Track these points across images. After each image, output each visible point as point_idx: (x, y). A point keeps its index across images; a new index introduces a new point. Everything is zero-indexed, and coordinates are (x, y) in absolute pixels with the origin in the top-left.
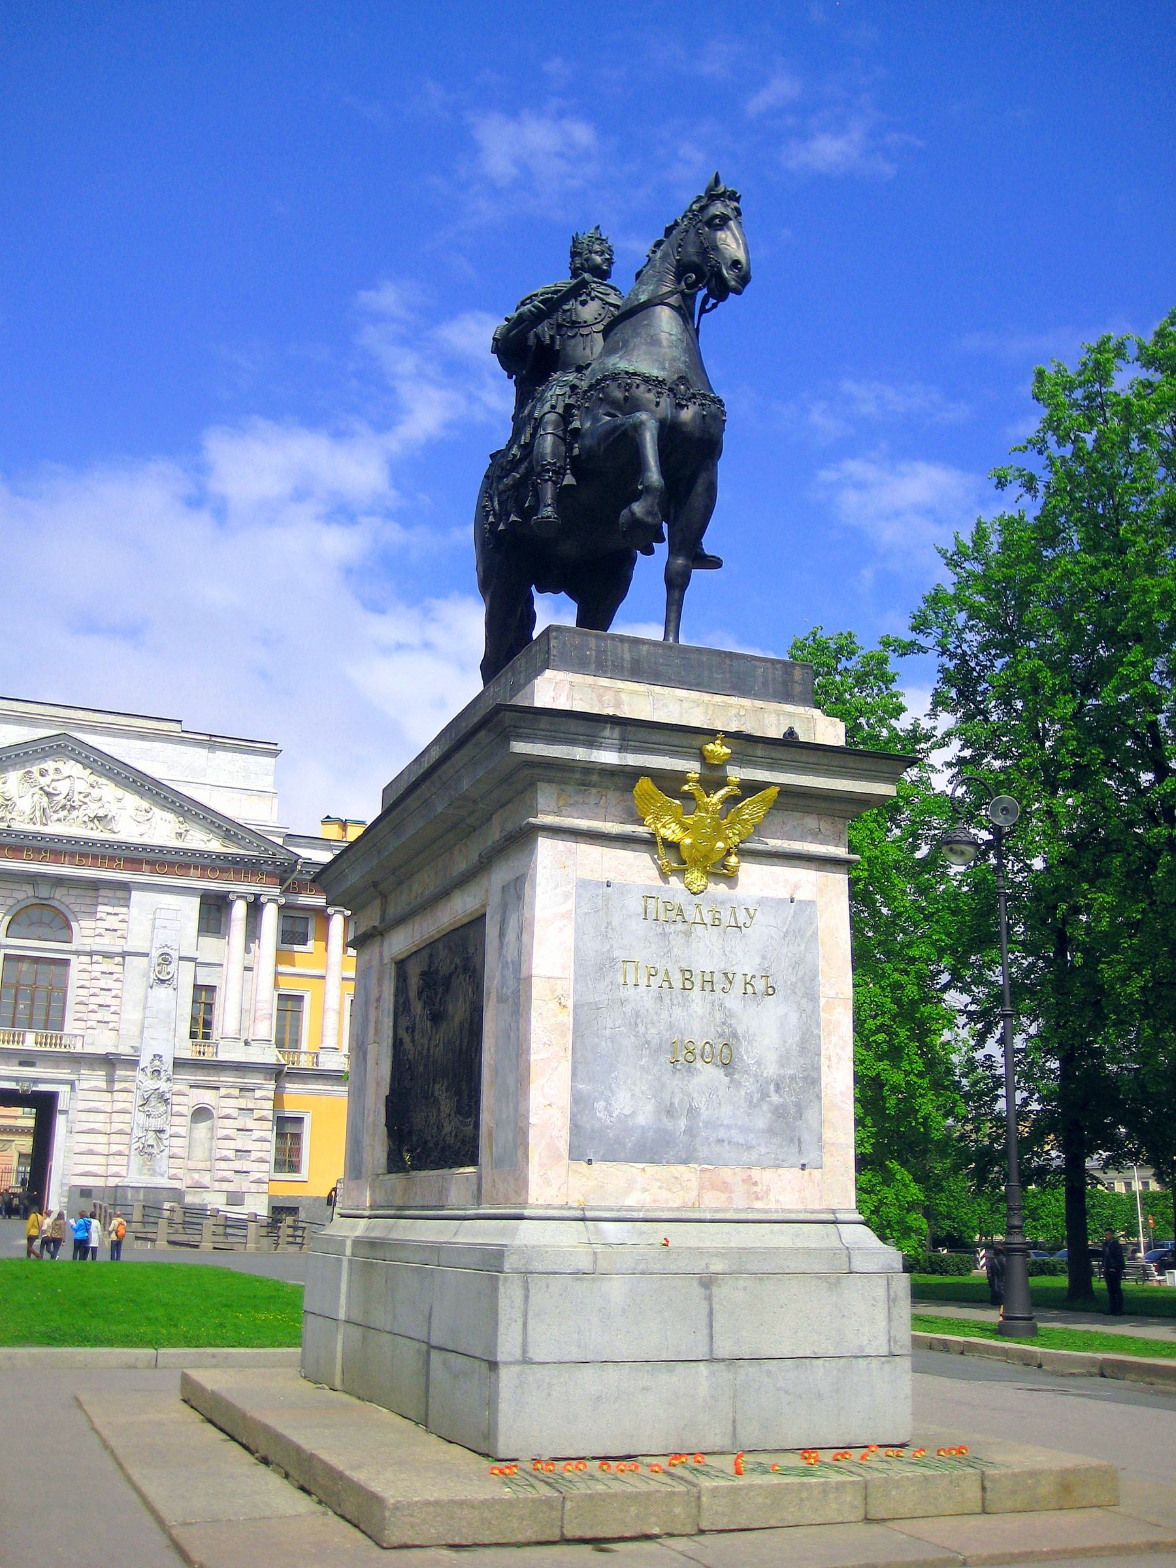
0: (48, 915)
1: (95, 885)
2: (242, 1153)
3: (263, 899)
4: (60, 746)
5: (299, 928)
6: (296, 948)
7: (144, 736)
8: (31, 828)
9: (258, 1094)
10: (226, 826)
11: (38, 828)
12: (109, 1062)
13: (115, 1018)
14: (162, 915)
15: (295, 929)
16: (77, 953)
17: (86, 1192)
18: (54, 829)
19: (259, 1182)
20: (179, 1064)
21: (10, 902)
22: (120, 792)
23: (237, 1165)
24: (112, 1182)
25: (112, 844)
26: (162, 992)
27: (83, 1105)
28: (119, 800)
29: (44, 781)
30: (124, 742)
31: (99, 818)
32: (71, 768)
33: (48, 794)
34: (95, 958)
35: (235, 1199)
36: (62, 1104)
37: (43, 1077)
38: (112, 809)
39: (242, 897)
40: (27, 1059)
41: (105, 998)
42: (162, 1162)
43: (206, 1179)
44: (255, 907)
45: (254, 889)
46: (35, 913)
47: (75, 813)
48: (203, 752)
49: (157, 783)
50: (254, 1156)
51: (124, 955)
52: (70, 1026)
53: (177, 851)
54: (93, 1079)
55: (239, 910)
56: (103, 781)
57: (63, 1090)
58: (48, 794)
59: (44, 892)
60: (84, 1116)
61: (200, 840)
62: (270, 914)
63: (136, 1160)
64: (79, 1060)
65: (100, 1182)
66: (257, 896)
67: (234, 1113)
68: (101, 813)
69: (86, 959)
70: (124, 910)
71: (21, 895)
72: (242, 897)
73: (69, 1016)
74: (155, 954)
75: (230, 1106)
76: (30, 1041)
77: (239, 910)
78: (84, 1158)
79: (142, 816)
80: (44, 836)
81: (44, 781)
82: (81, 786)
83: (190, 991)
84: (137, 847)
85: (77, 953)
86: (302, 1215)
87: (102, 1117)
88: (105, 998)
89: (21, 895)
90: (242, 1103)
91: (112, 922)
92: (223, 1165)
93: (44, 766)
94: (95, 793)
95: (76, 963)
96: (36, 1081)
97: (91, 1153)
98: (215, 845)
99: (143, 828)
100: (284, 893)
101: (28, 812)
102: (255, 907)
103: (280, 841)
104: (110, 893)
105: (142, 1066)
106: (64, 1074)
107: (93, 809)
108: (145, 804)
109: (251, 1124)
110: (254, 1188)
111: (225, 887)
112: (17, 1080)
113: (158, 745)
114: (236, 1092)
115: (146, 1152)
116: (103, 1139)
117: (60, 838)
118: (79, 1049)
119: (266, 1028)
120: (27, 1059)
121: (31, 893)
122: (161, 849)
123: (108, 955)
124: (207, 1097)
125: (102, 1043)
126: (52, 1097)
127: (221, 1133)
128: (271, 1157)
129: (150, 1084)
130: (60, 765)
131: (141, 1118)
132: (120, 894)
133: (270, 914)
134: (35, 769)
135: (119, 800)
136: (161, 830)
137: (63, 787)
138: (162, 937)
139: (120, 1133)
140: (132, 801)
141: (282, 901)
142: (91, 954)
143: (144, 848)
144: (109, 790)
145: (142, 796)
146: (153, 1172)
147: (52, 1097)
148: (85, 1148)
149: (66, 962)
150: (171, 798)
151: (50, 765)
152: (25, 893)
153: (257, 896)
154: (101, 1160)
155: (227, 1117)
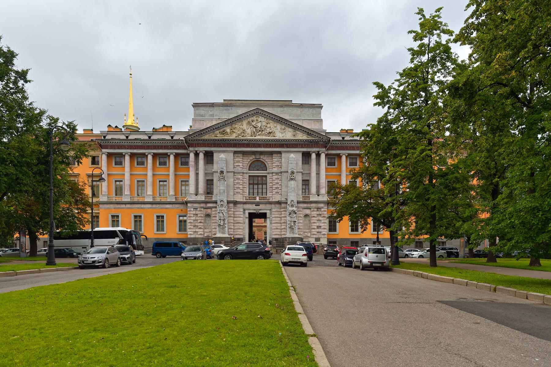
0: (260, 163)
1: (271, 153)
2: (319, 227)
4: (258, 112)
9: (322, 210)
11: (253, 138)
12: (279, 203)
16: (268, 173)
19: (324, 235)
20: (298, 202)
21: (249, 160)
22: (275, 125)
23: (318, 230)
24: (283, 236)
25: (274, 140)
26: (292, 182)
27: (273, 216)
29: (253, 124)
30: (275, 109)
31: (270, 133)
32: (261, 119)
33: (255, 127)
36: (268, 216)
37: (262, 209)
38: (273, 130)
39: (314, 152)
42: (296, 231)
43: (309, 235)
44: (318, 155)
45: (317, 149)
46: (256, 163)
49: (286, 120)
51: (281, 172)
52: (269, 195)
53: (294, 140)
54: (275, 208)
55: (314, 156)
56: (271, 121)
57: (268, 212)
58: (255, 127)
60: (274, 219)
61: (301, 136)
62: (323, 156)
63: (288, 230)
64: (271, 203)
65: (280, 237)
66: (319, 152)
67: (316, 215)
68: (270, 131)
69: (271, 175)
71: (251, 158)
72: (314, 152)
74: (289, 171)
75: (315, 213)
77: (314, 156)
79: (282, 131)
80: (255, 140)
81: (253, 124)
82: (264, 124)
83: (301, 182)
84: (282, 140)
85: (268, 173)
89: (251, 158)
90: (318, 213)
92: (313, 230)
93: (253, 119)
94: (268, 126)
96: (260, 210)
97: (277, 229)
102: (318, 155)
104: (276, 155)
107: (268, 130)
108: (283, 127)
109: (321, 218)
110: (323, 236)
111: (309, 150)
112: (255, 210)
113: (285, 109)
114: (316, 210)
115: (291, 228)
117: (260, 140)
119: (323, 191)
120: (257, 204)
122: (289, 140)
123: (277, 174)
124: (308, 212)
125: (277, 198)
127: (312, 221)
128: (327, 227)
129: (291, 209)
130: (257, 118)
131: (288, 218)
132: (279, 155)
133: (323, 156)
136: (288, 135)
137: (259, 125)
138: (291, 166)
139: (284, 223)
140: (279, 126)
141: (326, 152)
142: (272, 173)
143: (284, 140)
145: (282, 125)
146: (293, 233)
148: (275, 227)
150: (290, 124)
151: (254, 118)
152: (252, 158)
155: (314, 217)
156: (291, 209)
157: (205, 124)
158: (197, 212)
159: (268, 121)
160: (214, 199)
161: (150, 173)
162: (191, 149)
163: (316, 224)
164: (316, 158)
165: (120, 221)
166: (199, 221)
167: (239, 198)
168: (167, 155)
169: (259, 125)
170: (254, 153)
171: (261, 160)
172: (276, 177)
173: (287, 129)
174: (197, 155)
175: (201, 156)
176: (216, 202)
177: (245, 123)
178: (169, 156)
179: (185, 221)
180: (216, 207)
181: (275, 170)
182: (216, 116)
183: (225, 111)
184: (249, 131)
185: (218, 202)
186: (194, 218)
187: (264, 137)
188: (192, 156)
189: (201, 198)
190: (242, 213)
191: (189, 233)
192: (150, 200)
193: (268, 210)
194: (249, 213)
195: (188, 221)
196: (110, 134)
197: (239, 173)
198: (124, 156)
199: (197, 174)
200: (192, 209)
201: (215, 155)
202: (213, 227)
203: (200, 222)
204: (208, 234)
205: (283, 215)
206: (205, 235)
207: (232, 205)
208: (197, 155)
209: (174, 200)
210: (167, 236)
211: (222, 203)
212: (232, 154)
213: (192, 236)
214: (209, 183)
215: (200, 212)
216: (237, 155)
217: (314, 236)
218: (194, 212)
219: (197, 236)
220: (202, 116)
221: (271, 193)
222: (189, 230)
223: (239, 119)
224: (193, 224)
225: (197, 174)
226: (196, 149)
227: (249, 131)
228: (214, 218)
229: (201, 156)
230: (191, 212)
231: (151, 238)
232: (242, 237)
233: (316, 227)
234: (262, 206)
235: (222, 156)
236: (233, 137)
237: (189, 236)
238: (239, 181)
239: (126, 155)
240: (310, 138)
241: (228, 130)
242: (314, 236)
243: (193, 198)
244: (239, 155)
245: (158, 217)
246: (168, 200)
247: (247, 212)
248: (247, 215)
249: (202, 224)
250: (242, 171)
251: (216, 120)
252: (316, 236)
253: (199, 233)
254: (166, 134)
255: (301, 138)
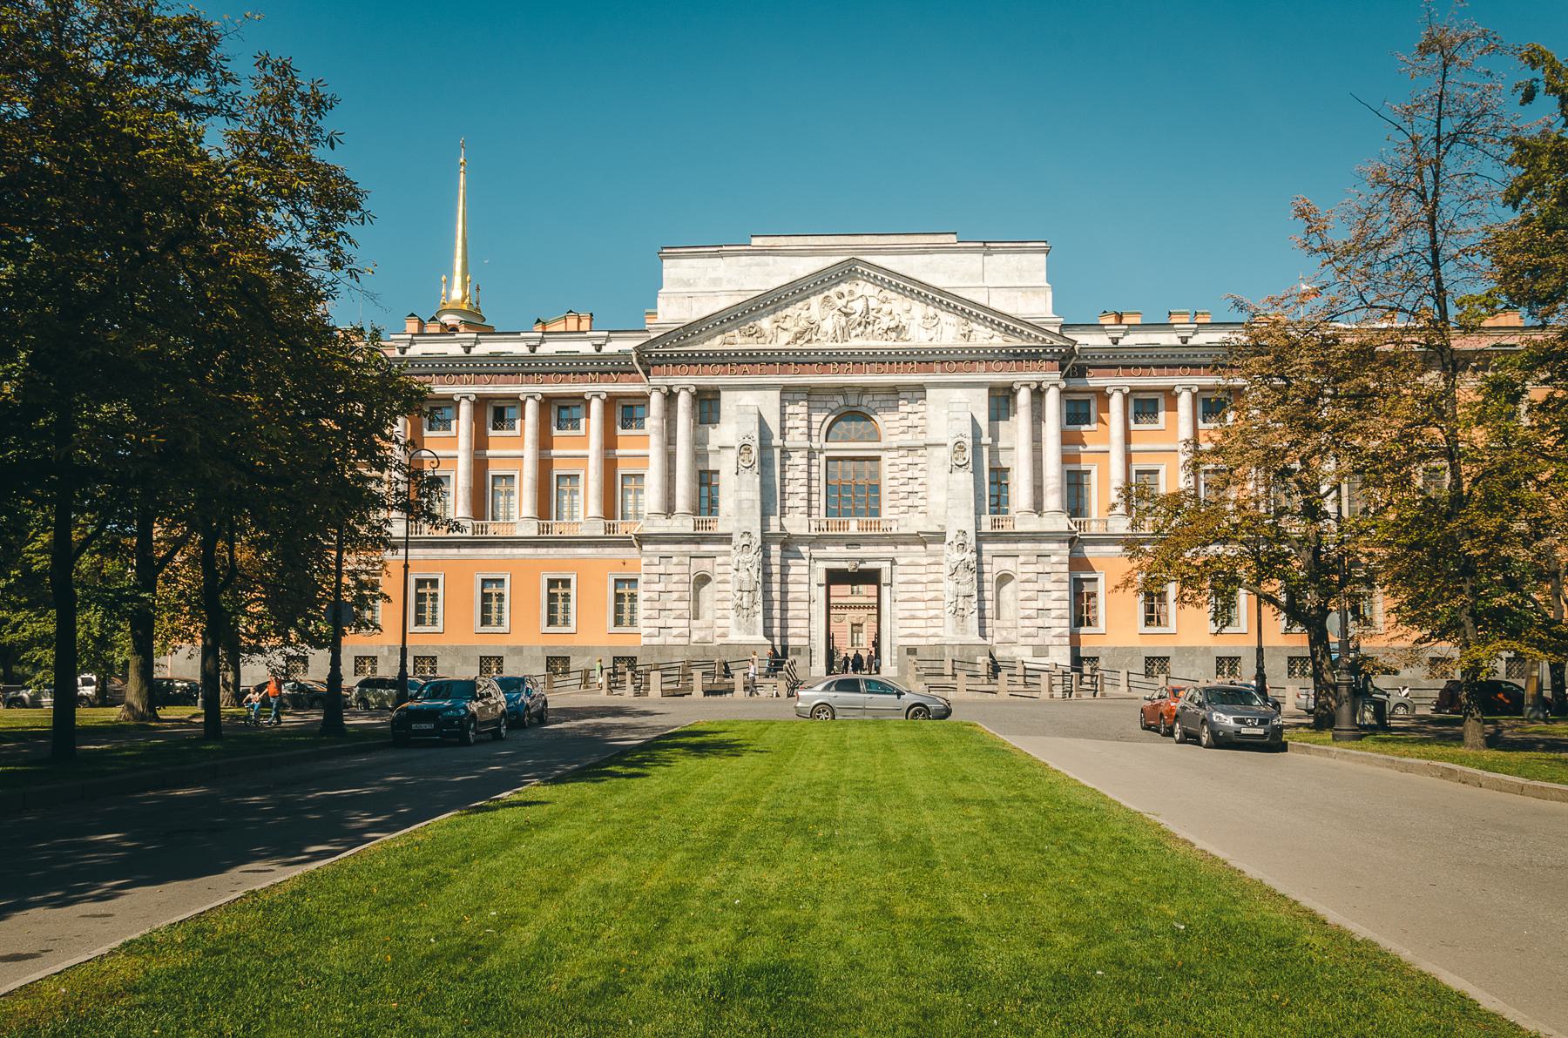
1: (895, 391)
3: (1044, 386)
5: (1082, 410)
6: (1085, 428)
7: (925, 251)
8: (834, 345)
9: (1054, 559)
10: (1004, 322)
12: (922, 539)
13: (923, 502)
14: (952, 410)
15: (1078, 412)
17: (912, 651)
18: (855, 343)
23: (1040, 622)
28: (908, 311)
32: (864, 288)
33: (846, 315)
34: (901, 453)
35: (1041, 651)
36: (885, 578)
40: (853, 542)
41: (914, 486)
43: (1013, 637)
44: (1038, 394)
47: (870, 328)
48: (978, 257)
49: (940, 291)
50: (1054, 613)
51: (926, 446)
52: (886, 513)
55: (1023, 397)
56: (894, 295)
57: (885, 566)
58: (846, 315)
59: (853, 401)
60: (904, 587)
61: (984, 337)
62: (1052, 400)
63: (950, 621)
65: (922, 642)
66: (1040, 384)
68: (893, 325)
69: (894, 454)
70: (922, 408)
73: (885, 504)
74: (951, 443)
76: (854, 527)
77: (1023, 397)
78: (908, 623)
86: (1102, 664)
87: (919, 587)
88: (914, 486)
89: (834, 405)
91: (913, 420)
92: (1027, 622)
94: (886, 308)
95: (886, 457)
96: (862, 561)
97: (913, 618)
98: (999, 340)
99: (932, 333)
100: (1066, 377)
101: (831, 332)
102: (1038, 394)
103: (1057, 330)
105: (948, 540)
106: (887, 551)
107: (886, 322)
108: (931, 311)
109: (1049, 586)
110: (1056, 641)
112: (846, 560)
116: (921, 605)
118: (894, 531)
119: (1052, 500)
120: (853, 542)
121: (842, 402)
123: (912, 449)
126: (877, 572)
130: (853, 287)
131: (949, 586)
132: (917, 395)
133: (1052, 400)
134: (832, 293)
135: (908, 311)
136: (948, 332)
140: (919, 309)
141: (1063, 385)
143: (933, 350)
144: (898, 304)
146: (964, 631)
147: (877, 572)
148: (907, 614)
149: (878, 459)
150: (953, 303)
153: (1040, 384)
154: (922, 623)
156: (957, 556)
157: (696, 306)
158: (671, 569)
159: (887, 293)
160: (720, 528)
161: (529, 452)
162: (655, 381)
163: (1034, 604)
164: (1033, 403)
165: (441, 597)
166: (675, 596)
167: (796, 524)
168: (582, 401)
169: (858, 306)
170: (841, 390)
171: (864, 409)
172: (909, 460)
173: (943, 316)
174: (670, 397)
175: (683, 401)
176: (726, 539)
177: (815, 301)
178: (588, 402)
179: (633, 597)
180: (727, 553)
181: (908, 439)
182: (729, 282)
183: (754, 269)
184: (828, 326)
185: (736, 538)
186: (660, 587)
187: (873, 343)
188: (656, 401)
189: (683, 524)
190: (805, 570)
191: (645, 631)
192: (530, 530)
193: (886, 559)
194: (829, 572)
195: (642, 595)
196: (421, 342)
197: (796, 449)
198: (458, 403)
199: (670, 458)
200: (656, 560)
201: (725, 396)
202: (719, 613)
203: (680, 600)
204: (702, 634)
205: (932, 577)
206: (695, 638)
207: (775, 549)
208: (670, 397)
209: (602, 533)
210: (578, 641)
211: (745, 541)
212: (776, 394)
213: (656, 641)
214: (705, 480)
215: (678, 569)
216: (790, 396)
217: (1030, 641)
218: (661, 569)
219: (670, 641)
220: (688, 283)
221: (895, 510)
222: (641, 622)
223: (797, 291)
224: (657, 605)
225: (670, 458)
226: (670, 382)
227: (828, 326)
228: (721, 587)
229: (683, 401)
230: (654, 569)
231: (530, 648)
232: (805, 642)
233: (1033, 613)
234: (865, 551)
235: (748, 398)
236: (782, 341)
237: (645, 641)
238: (798, 475)
239: (464, 401)
240: (1015, 342)
241: (766, 323)
242: (1030, 641)
243: (662, 526)
244: (797, 396)
245: (552, 583)
246: (585, 533)
247: (821, 567)
248: (821, 577)
249: (684, 605)
250: (807, 444)
251: (730, 293)
252: (1036, 641)
253: (675, 632)
254: (581, 339)
255: (986, 343)
